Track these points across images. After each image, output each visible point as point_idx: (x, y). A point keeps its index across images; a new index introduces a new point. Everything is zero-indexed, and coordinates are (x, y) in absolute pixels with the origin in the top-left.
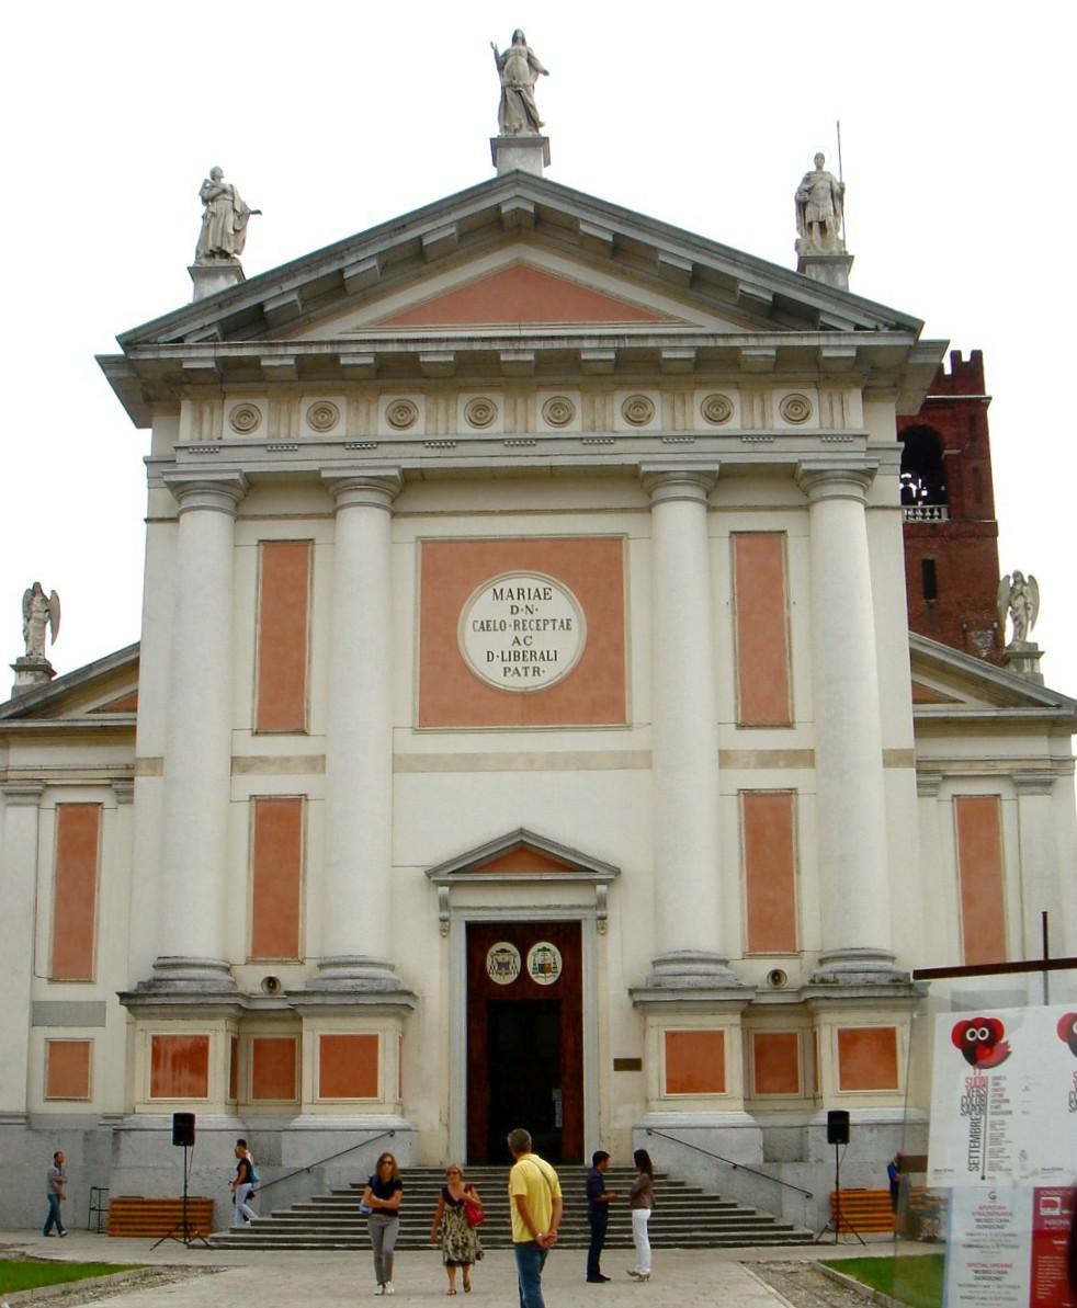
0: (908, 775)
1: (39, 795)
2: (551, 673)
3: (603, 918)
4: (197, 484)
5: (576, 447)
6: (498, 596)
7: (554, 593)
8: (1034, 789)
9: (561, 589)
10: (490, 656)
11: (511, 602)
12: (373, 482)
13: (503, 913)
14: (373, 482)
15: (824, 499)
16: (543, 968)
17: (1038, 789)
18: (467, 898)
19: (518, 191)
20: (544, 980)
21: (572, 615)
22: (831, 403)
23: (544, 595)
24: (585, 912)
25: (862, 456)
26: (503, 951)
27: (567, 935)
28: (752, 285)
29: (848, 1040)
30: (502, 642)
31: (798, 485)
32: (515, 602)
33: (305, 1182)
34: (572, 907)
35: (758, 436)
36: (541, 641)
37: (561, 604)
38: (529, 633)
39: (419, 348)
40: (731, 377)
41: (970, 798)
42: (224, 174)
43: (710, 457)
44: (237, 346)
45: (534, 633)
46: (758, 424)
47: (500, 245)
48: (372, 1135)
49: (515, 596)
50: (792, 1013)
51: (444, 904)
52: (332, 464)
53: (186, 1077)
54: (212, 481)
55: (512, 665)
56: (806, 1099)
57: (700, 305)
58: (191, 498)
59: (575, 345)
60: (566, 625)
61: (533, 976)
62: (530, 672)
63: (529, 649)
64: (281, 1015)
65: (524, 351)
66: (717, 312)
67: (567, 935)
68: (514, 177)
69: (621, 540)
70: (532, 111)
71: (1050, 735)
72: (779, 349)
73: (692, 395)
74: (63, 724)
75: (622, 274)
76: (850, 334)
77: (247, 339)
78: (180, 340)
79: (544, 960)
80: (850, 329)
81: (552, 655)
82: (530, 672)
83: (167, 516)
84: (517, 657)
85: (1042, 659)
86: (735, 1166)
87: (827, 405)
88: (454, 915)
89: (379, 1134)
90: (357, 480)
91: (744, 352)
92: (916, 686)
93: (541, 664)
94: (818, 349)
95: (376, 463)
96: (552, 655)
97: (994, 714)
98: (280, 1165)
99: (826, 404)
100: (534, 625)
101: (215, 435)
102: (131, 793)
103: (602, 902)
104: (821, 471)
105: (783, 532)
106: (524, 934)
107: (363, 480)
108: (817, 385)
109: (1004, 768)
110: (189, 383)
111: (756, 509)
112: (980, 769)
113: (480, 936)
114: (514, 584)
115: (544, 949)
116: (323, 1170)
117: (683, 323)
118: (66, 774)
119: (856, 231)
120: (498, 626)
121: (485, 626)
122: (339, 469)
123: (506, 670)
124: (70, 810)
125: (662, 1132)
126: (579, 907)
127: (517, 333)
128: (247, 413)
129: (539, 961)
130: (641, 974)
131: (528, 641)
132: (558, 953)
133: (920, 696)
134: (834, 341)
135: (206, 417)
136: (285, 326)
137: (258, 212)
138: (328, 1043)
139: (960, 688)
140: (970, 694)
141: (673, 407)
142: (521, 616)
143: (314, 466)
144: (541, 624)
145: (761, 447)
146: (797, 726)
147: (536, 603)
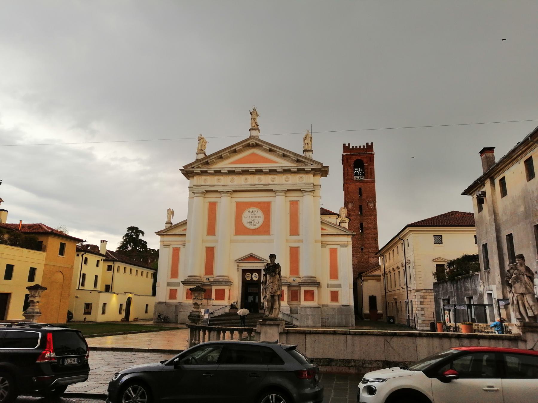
2: (258, 226)
6: (249, 212)
10: (247, 223)
11: (251, 213)
17: (345, 247)
19: (252, 140)
24: (262, 268)
26: (248, 274)
28: (293, 157)
29: (306, 292)
32: (252, 213)
34: (260, 267)
36: (256, 220)
37: (260, 213)
45: (255, 219)
51: (238, 266)
55: (251, 224)
78: (194, 167)
81: (258, 222)
86: (285, 314)
88: (240, 268)
96: (258, 222)
100: (255, 217)
102: (185, 246)
106: (252, 271)
113: (244, 271)
134: (307, 167)
138: (216, 290)
142: (253, 215)
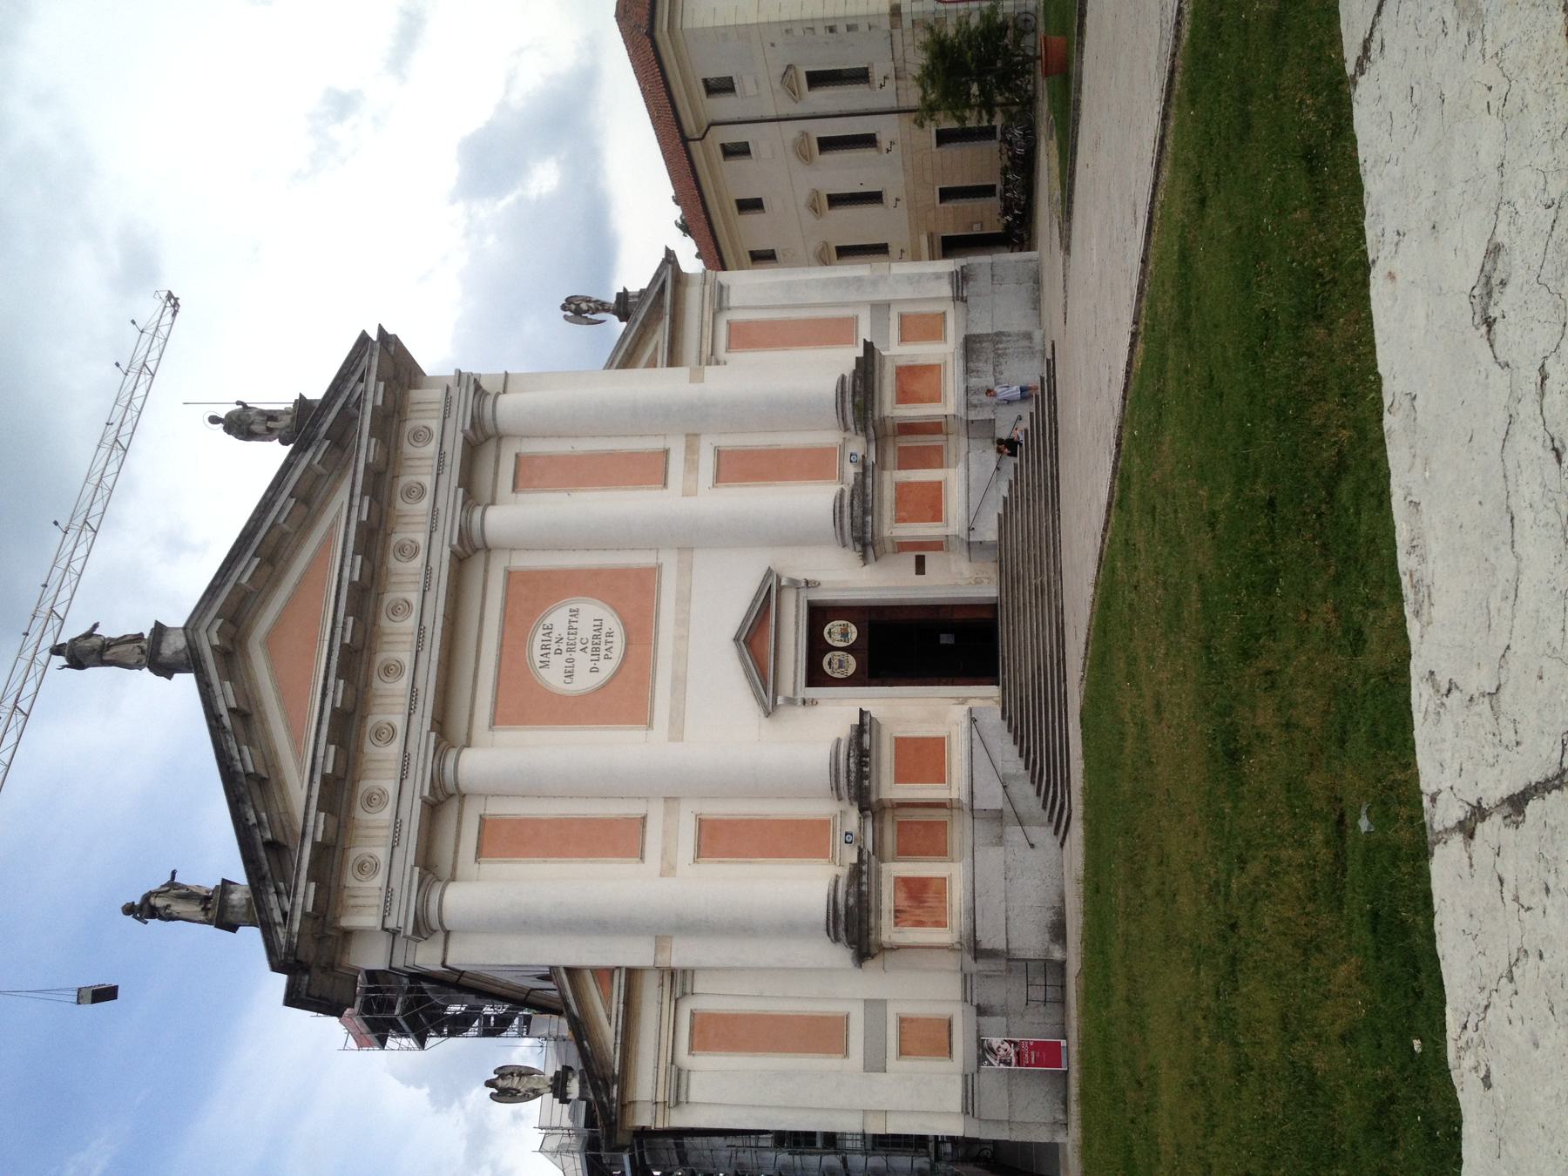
0: (710, 371)
1: (679, 1070)
2: (612, 622)
3: (807, 582)
4: (419, 905)
5: (430, 596)
6: (545, 665)
7: (547, 622)
8: (725, 297)
9: (545, 617)
10: (594, 670)
11: (552, 656)
12: (438, 754)
13: (800, 658)
14: (438, 754)
15: (494, 419)
16: (845, 634)
17: (725, 293)
18: (787, 688)
19: (202, 631)
20: (853, 633)
21: (568, 607)
22: (418, 411)
23: (549, 630)
24: (801, 598)
25: (463, 390)
26: (830, 663)
27: (819, 615)
28: (315, 455)
29: (904, 397)
30: (583, 661)
31: (482, 443)
32: (552, 651)
33: (1014, 789)
34: (797, 606)
35: (439, 462)
36: (585, 630)
37: (558, 618)
38: (578, 641)
39: (345, 584)
40: (380, 537)
41: (729, 340)
42: (130, 901)
43: (452, 494)
44: (298, 874)
45: (579, 637)
46: (429, 462)
47: (246, 656)
48: (976, 735)
49: (547, 651)
50: (884, 450)
51: (791, 701)
52: (417, 788)
53: (930, 896)
54: (418, 890)
55: (603, 653)
56: (947, 440)
57: (324, 504)
58: (486, 410)
59: (345, 584)
60: (574, 612)
61: (851, 642)
62: (610, 639)
63: (591, 640)
64: (877, 830)
65: (345, 623)
66: (333, 490)
67: (819, 615)
68: (189, 631)
69: (510, 573)
70: (128, 638)
71: (686, 285)
72: (371, 435)
73: (399, 510)
74: (618, 1059)
75: (288, 562)
76: (366, 386)
77: (293, 865)
78: (284, 915)
79: (839, 633)
80: (362, 386)
81: (598, 623)
82: (610, 639)
83: (442, 946)
84: (597, 650)
85: (629, 290)
86: (998, 469)
87: (421, 414)
88: (800, 696)
89: (974, 730)
90: (435, 766)
91: (371, 460)
92: (647, 366)
93: (605, 630)
94: (374, 408)
95: (422, 756)
96: (598, 623)
97: (668, 317)
98: (1001, 810)
99: (416, 415)
100: (572, 637)
101: (378, 893)
102: (684, 971)
103: (794, 583)
104: (473, 417)
105: (517, 455)
106: (817, 648)
107: (464, 514)
108: (402, 421)
109: (708, 316)
110: (325, 916)
111: (496, 474)
112: (708, 332)
113: (816, 676)
114: (537, 652)
115: (829, 633)
116: (1004, 775)
117: (338, 516)
118: (705, 333)
119: (277, 396)
120: (570, 665)
121: (569, 674)
122: (423, 780)
123: (607, 658)
124: (696, 1041)
125: (971, 519)
126: (797, 601)
127: (326, 644)
128: (402, 549)
129: (839, 637)
130: (851, 556)
131: (584, 641)
132: (835, 623)
133: (652, 364)
134: (370, 396)
135: (359, 901)
136: (288, 833)
137: (174, 873)
138: (900, 778)
139: (646, 344)
140: (651, 338)
141: (400, 583)
142: (564, 647)
143: (418, 803)
144: (572, 631)
145: (448, 461)
146: (667, 447)
147: (554, 636)
